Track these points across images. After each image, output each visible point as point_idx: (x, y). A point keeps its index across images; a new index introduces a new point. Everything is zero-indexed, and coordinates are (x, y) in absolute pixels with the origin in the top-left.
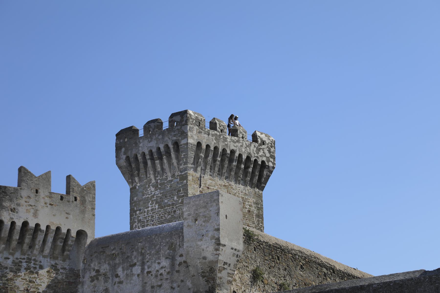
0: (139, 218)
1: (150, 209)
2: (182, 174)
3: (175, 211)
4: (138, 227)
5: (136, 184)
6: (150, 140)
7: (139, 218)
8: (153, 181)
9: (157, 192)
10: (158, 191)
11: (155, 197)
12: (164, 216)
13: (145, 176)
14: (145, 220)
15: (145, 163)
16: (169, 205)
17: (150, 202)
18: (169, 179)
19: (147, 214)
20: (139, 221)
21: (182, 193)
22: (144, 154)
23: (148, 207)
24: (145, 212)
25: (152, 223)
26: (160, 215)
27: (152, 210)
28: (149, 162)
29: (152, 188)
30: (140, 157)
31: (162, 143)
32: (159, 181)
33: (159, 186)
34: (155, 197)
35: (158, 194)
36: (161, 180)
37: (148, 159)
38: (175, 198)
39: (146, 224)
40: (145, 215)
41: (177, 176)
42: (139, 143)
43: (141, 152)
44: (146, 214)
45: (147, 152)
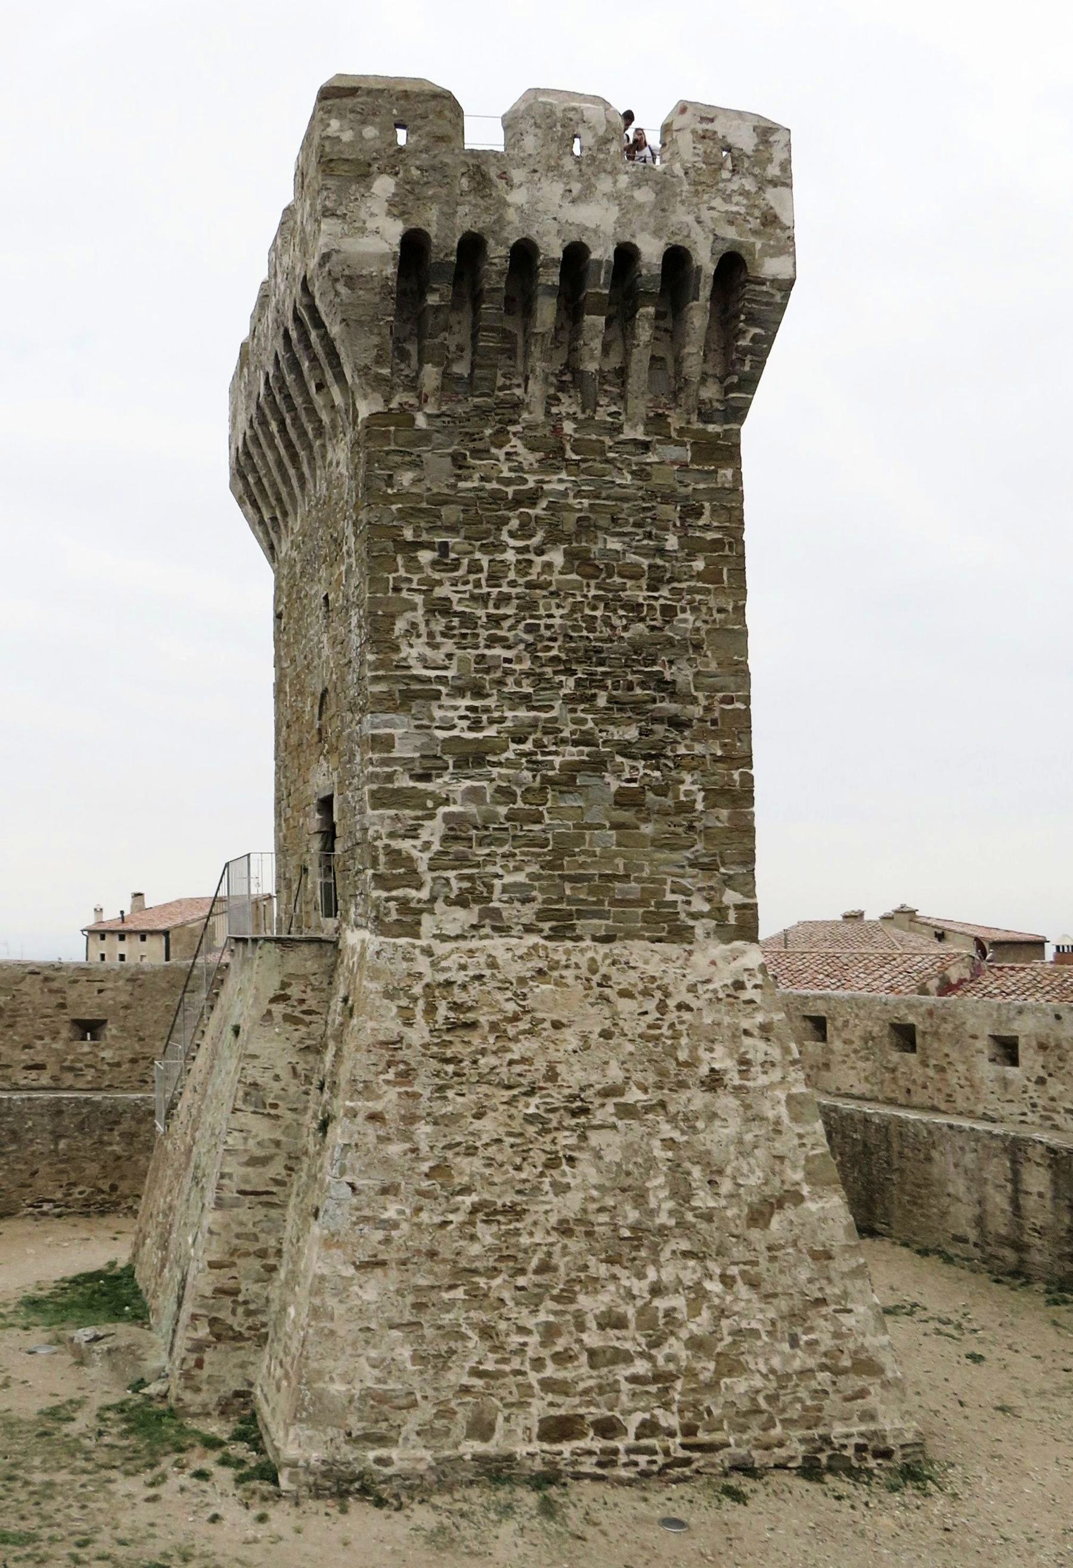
7: (439, 592)
8: (535, 414)
9: (558, 482)
10: (563, 475)
11: (544, 504)
16: (634, 574)
17: (514, 524)
18: (628, 434)
19: (494, 579)
20: (440, 608)
23: (502, 547)
24: (475, 567)
25: (530, 638)
26: (576, 607)
29: (521, 449)
32: (568, 427)
35: (564, 494)
36: (581, 425)
39: (484, 633)
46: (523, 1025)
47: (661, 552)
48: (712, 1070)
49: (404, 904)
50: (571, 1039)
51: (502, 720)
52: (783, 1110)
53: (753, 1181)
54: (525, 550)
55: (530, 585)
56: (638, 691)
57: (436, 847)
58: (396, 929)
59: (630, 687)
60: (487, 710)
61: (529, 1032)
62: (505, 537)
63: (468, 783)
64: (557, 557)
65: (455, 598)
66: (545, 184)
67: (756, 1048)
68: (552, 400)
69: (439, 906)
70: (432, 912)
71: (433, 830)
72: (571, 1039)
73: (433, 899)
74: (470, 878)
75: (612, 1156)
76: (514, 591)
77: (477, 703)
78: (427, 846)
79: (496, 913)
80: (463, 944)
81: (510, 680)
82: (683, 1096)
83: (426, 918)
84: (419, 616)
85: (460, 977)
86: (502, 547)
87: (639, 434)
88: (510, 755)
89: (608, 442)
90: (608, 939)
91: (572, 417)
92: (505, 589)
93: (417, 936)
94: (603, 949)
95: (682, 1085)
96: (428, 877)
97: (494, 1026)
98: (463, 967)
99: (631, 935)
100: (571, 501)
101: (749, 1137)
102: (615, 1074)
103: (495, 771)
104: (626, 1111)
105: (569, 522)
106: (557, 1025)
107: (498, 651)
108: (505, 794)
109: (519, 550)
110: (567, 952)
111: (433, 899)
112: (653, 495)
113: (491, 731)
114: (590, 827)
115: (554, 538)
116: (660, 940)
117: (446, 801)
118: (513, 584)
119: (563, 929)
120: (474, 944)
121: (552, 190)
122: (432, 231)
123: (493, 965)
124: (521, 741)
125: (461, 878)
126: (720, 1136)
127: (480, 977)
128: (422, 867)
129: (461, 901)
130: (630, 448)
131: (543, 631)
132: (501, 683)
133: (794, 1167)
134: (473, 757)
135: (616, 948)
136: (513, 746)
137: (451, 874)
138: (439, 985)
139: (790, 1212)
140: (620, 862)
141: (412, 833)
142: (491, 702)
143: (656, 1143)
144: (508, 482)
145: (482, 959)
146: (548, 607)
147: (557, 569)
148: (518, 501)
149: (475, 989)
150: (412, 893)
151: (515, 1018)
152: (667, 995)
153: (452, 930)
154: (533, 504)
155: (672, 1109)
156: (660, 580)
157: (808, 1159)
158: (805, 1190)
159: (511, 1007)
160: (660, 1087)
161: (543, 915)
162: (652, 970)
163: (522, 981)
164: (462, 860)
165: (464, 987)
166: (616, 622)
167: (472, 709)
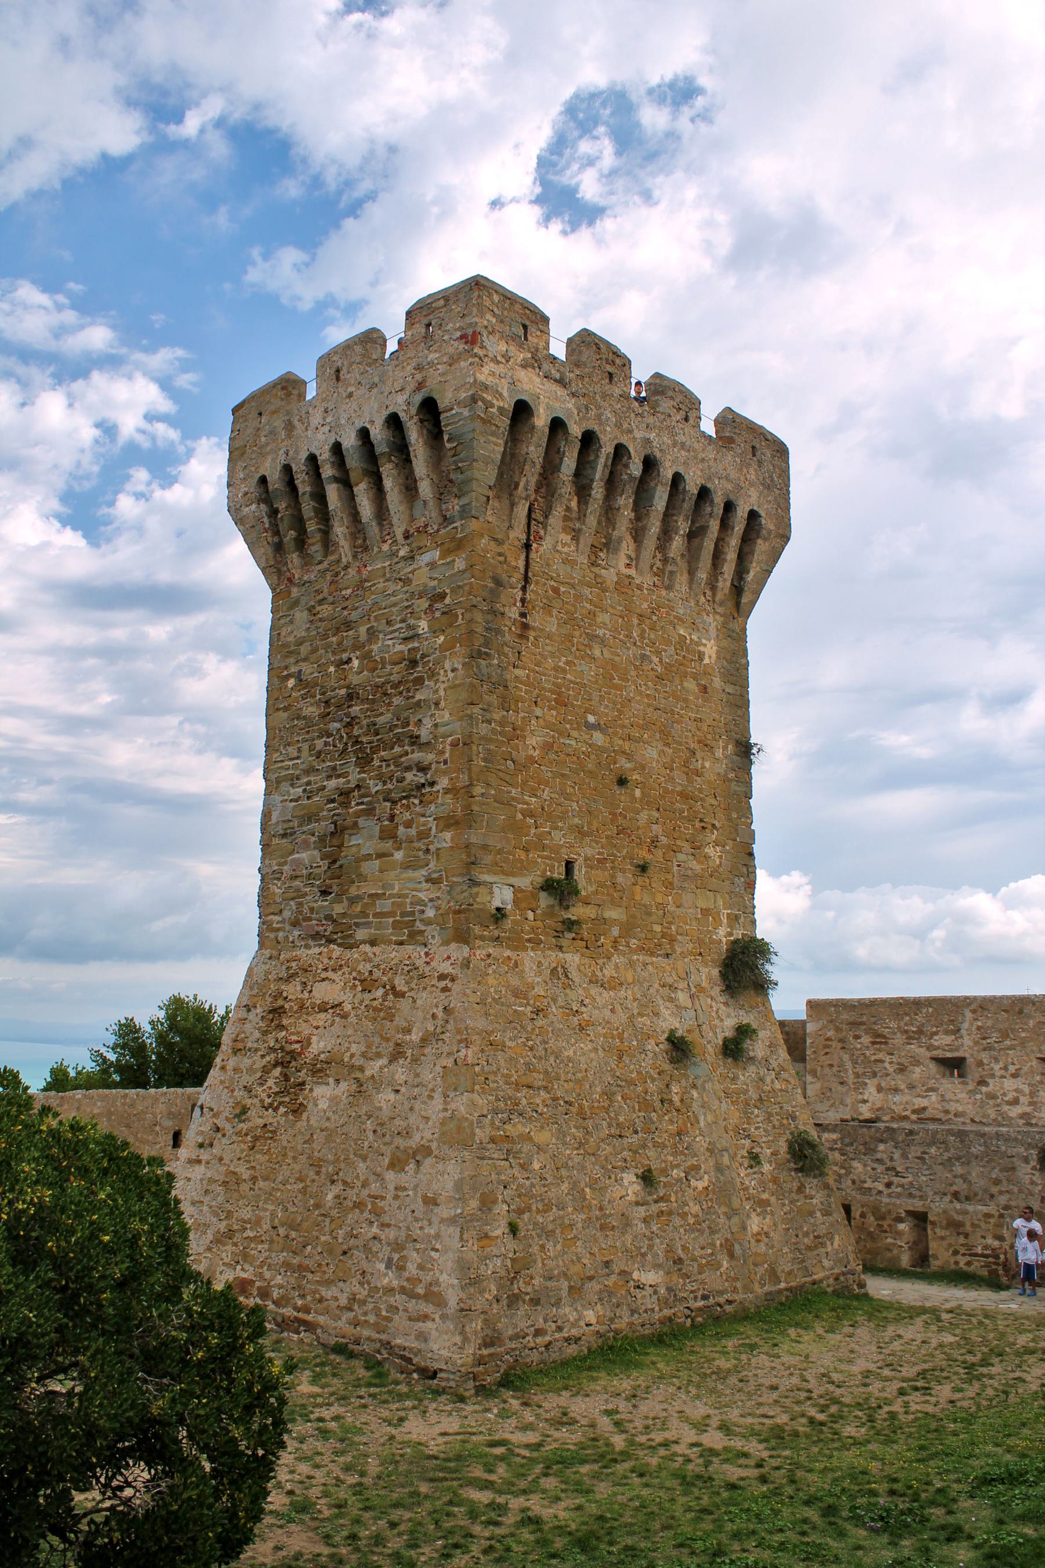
15: (320, 497)
43: (304, 455)
45: (324, 455)
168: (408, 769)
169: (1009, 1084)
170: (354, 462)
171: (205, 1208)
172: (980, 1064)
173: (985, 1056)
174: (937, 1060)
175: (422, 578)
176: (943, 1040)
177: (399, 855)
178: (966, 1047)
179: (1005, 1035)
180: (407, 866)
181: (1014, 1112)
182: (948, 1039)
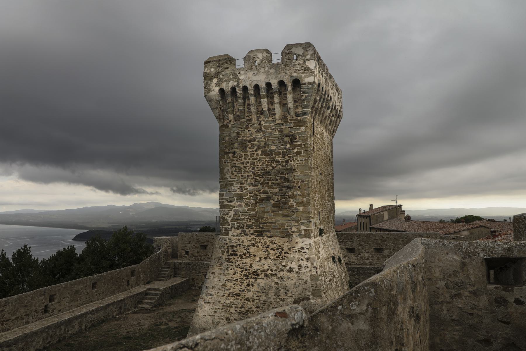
0: (234, 162)
1: (249, 153)
2: (299, 118)
3: (287, 162)
4: (232, 172)
5: (228, 121)
6: (256, 72)
9: (259, 135)
10: (262, 134)
11: (257, 140)
12: (271, 166)
13: (243, 114)
14: (242, 166)
16: (278, 154)
17: (250, 146)
18: (277, 122)
19: (245, 159)
21: (298, 141)
22: (245, 89)
23: (247, 151)
24: (241, 156)
25: (253, 171)
26: (263, 163)
27: (252, 155)
28: (252, 99)
30: (239, 92)
31: (275, 78)
32: (263, 123)
33: (263, 129)
34: (257, 140)
35: (261, 138)
36: (266, 122)
37: (252, 95)
38: (288, 146)
39: (243, 170)
40: (241, 160)
41: (291, 120)
42: (239, 75)
43: (241, 85)
44: (243, 158)
46: (247, 255)
47: (286, 148)
48: (290, 268)
49: (226, 230)
50: (257, 259)
51: (247, 189)
52: (308, 278)
53: (297, 293)
54: (253, 151)
55: (253, 159)
56: (279, 181)
57: (232, 217)
58: (224, 234)
59: (277, 180)
60: (244, 187)
61: (248, 257)
62: (248, 149)
63: (239, 203)
64: (259, 152)
65: (237, 163)
66: (248, 73)
67: (304, 263)
68: (258, 118)
69: (233, 229)
70: (231, 231)
71: (232, 213)
72: (257, 259)
73: (231, 228)
74: (239, 223)
75: (262, 285)
76: (249, 161)
77: (242, 186)
78: (230, 216)
79: (244, 231)
80: (238, 238)
81: (249, 180)
82: (282, 273)
83: (231, 233)
84: (229, 168)
85: (235, 245)
86: (247, 151)
87: (280, 122)
88: (248, 196)
89: (272, 125)
90: (270, 237)
91: (263, 120)
92: (248, 160)
93: (228, 236)
94: (269, 239)
95: (282, 270)
96: (231, 223)
97: (240, 255)
98: (236, 243)
99: (276, 236)
100: (263, 139)
101: (297, 284)
102: (266, 267)
103: (245, 200)
104: (266, 276)
105: (262, 144)
106: (255, 256)
107: (246, 174)
108: (247, 205)
109: (251, 152)
110: (260, 240)
111: (231, 228)
112: (284, 136)
113: (244, 191)
114: (266, 212)
115: (259, 147)
116: (284, 237)
117: (235, 207)
118: (249, 159)
119: (260, 235)
120: (239, 238)
121: (250, 74)
122: (224, 88)
123: (243, 242)
124: (252, 193)
125: (237, 223)
126: (288, 283)
127: (240, 245)
128: (229, 221)
129: (237, 228)
130: (278, 125)
131: (256, 169)
132: (247, 181)
133: (309, 292)
134: (240, 197)
135: (273, 239)
136: (249, 195)
137: (235, 222)
138: (231, 246)
139: (306, 302)
140: (274, 220)
141: (228, 214)
142: (245, 185)
143: (273, 283)
144: (249, 137)
145: (241, 241)
146: (257, 163)
147: (259, 154)
148: (250, 141)
149: (238, 248)
150: (227, 226)
151: (245, 254)
152: (283, 250)
153: (235, 234)
154: (255, 141)
155: (279, 276)
156: (285, 155)
157: (313, 290)
158: (311, 297)
159: (245, 251)
160: (276, 271)
161: (255, 231)
162: (280, 244)
163: (249, 246)
164: (237, 219)
165: (236, 247)
166: (273, 165)
167: (241, 187)
168: (283, 187)
169: (366, 255)
170: (263, 92)
171: (216, 317)
172: (359, 249)
173: (360, 248)
174: (347, 248)
175: (286, 132)
176: (349, 243)
177: (281, 212)
178: (355, 245)
179: (365, 242)
180: (284, 216)
181: (368, 261)
182: (350, 243)
